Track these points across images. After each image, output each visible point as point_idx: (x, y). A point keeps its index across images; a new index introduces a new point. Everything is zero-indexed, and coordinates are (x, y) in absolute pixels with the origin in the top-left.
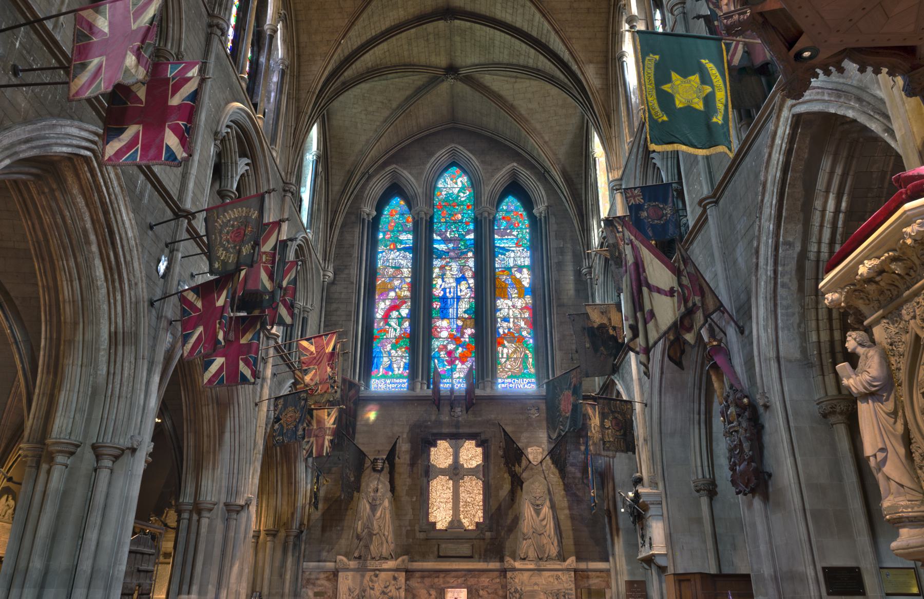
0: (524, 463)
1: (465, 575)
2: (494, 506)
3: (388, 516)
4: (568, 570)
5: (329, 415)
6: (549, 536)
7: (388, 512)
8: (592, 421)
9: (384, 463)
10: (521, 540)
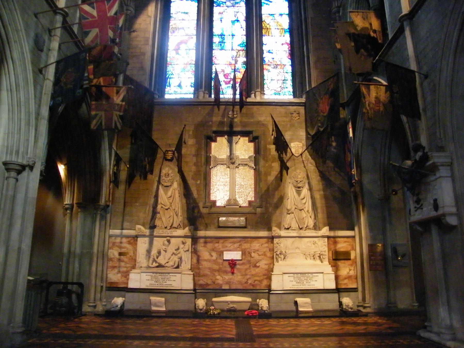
0: (289, 154)
1: (240, 241)
2: (263, 186)
3: (177, 195)
4: (323, 237)
5: (118, 92)
6: (308, 211)
7: (177, 192)
8: (366, 100)
9: (174, 154)
10: (285, 214)
